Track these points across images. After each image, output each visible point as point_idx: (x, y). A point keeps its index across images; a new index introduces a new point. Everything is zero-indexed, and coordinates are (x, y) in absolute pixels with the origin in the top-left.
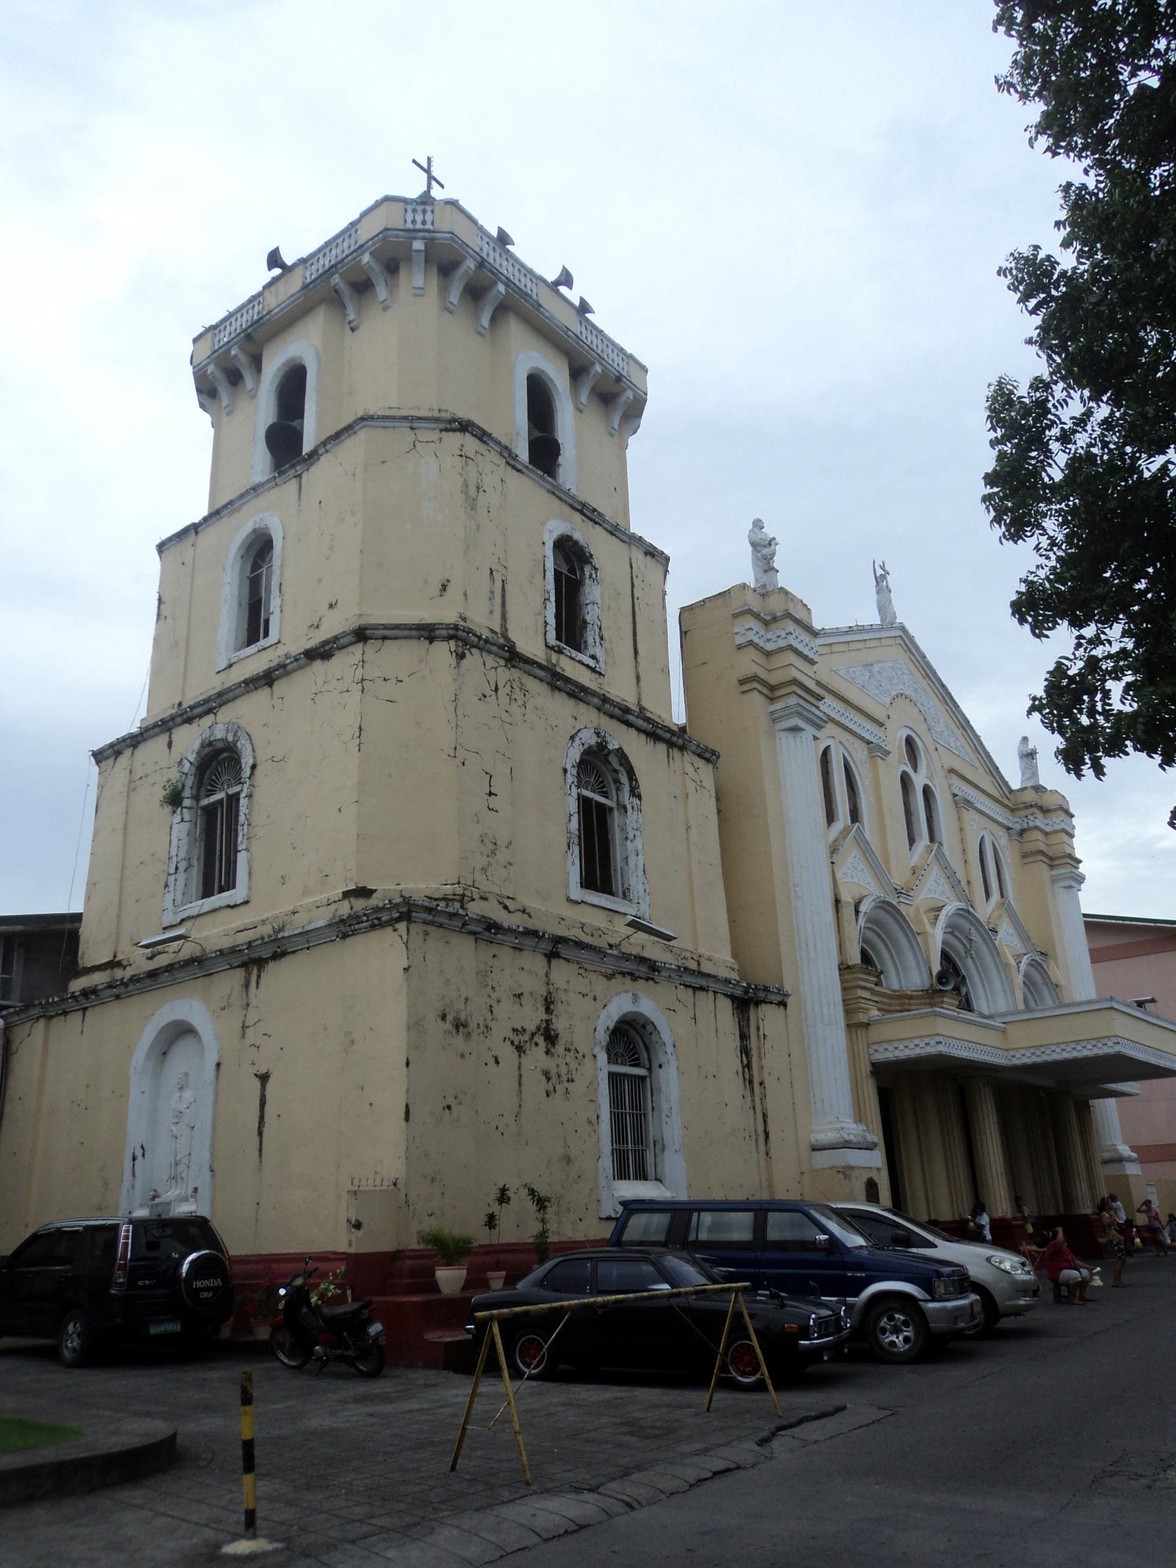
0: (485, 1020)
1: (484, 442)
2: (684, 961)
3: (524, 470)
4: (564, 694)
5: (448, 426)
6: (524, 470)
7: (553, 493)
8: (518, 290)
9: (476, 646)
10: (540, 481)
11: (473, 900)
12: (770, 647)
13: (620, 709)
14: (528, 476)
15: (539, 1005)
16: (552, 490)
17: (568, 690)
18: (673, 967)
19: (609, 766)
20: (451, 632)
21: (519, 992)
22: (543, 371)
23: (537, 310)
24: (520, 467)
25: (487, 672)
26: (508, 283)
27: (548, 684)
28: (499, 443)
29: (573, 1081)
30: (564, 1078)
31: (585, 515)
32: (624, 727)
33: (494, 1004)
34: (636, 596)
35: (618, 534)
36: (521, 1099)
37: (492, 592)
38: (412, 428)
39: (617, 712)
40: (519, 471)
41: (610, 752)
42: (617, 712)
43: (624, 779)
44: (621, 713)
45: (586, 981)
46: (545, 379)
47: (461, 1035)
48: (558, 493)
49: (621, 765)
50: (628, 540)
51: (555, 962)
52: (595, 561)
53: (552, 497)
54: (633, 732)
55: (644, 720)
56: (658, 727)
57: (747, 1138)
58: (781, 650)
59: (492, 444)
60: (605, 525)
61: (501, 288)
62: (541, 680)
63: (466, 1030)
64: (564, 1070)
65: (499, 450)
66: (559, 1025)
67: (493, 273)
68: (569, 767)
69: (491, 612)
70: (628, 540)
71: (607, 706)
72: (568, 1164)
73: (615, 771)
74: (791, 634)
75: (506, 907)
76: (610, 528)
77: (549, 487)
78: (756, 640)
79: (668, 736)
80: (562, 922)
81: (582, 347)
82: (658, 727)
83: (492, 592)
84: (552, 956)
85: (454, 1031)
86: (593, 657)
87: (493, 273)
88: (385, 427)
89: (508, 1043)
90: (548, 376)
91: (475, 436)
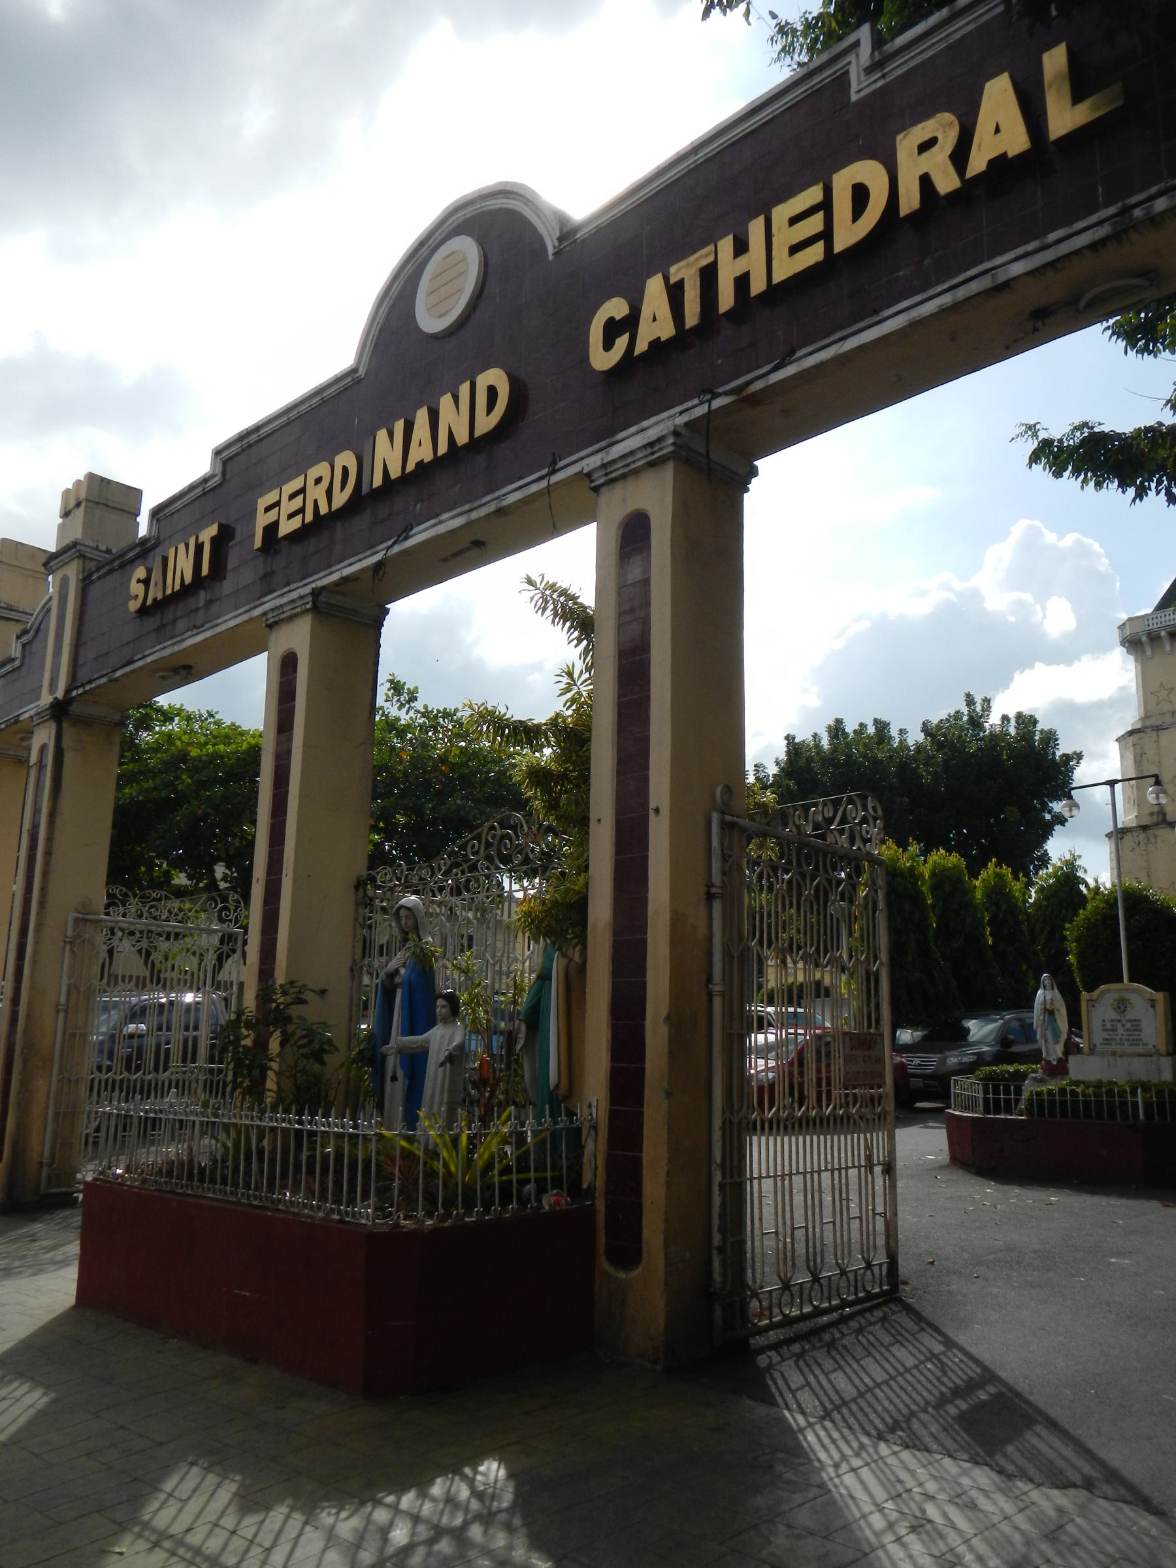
61: (1163, 634)
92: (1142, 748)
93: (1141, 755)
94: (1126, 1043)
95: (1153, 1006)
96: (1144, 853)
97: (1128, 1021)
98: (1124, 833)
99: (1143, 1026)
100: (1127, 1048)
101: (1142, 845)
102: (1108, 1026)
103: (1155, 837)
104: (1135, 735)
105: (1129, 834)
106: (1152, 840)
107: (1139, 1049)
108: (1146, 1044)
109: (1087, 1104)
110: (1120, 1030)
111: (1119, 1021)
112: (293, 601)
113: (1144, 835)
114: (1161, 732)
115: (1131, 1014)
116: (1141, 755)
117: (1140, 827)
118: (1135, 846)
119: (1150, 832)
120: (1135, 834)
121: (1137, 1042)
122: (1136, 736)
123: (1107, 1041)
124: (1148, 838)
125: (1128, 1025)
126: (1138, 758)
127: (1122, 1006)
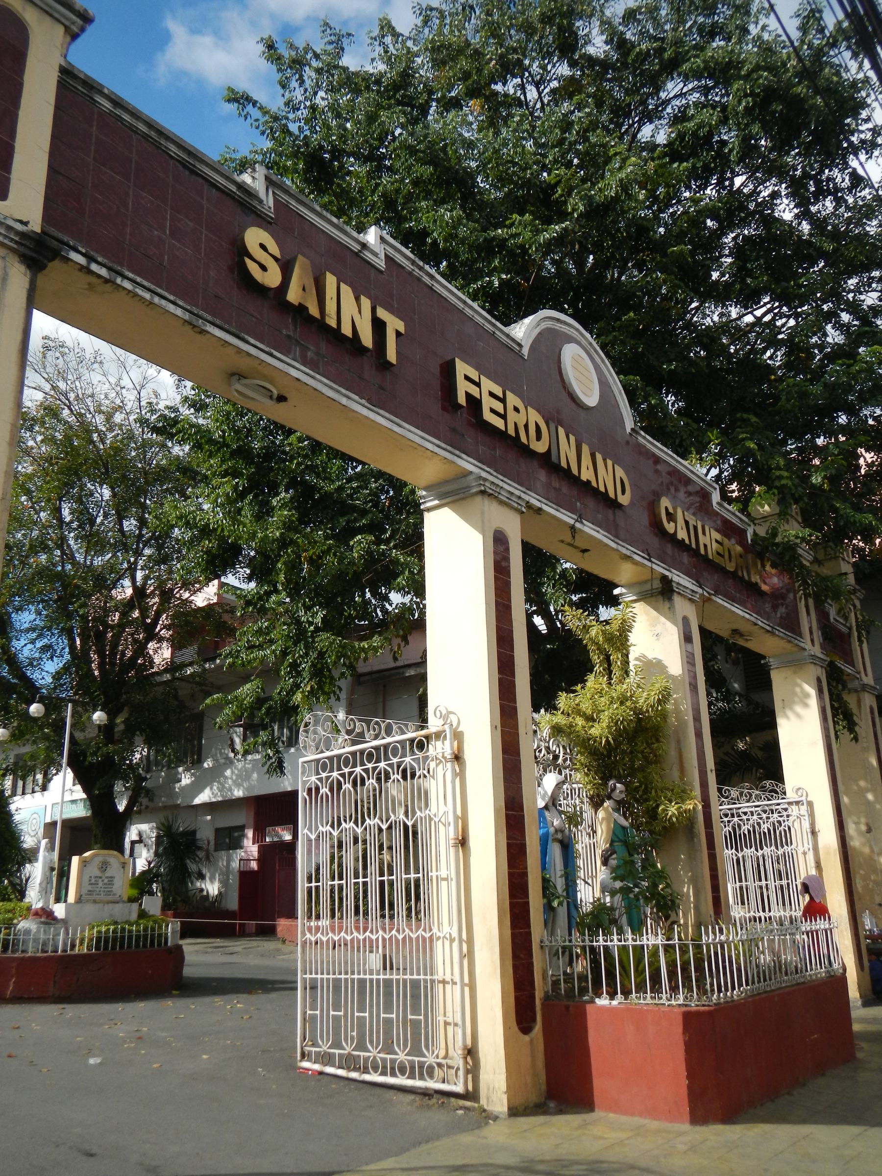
94: (102, 894)
95: (123, 867)
97: (107, 877)
99: (116, 881)
100: (102, 897)
102: (93, 881)
107: (110, 898)
108: (114, 895)
109: (138, 937)
110: (100, 884)
111: (100, 877)
112: (512, 494)
115: (109, 873)
121: (109, 893)
123: (90, 892)
125: (106, 881)
127: (104, 866)
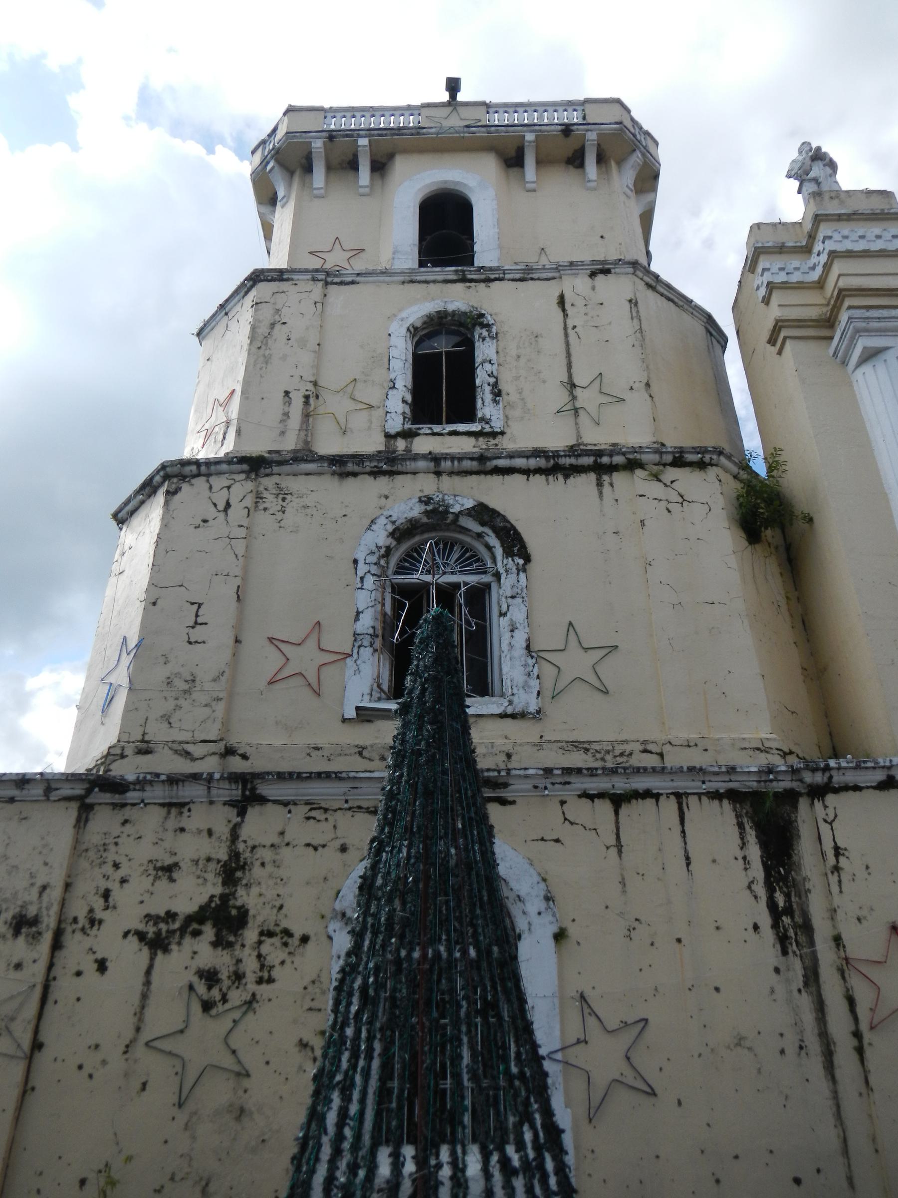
0: (91, 911)
1: (287, 280)
2: (620, 760)
3: (358, 279)
4: (367, 476)
5: (246, 289)
6: (358, 279)
7: (412, 282)
8: (384, 132)
9: (199, 475)
10: (388, 279)
11: (122, 756)
12: (815, 276)
13: (472, 459)
14: (367, 283)
15: (210, 876)
16: (408, 278)
17: (368, 469)
18: (531, 772)
19: (471, 533)
20: (162, 473)
21: (168, 861)
22: (446, 182)
23: (418, 134)
24: (349, 279)
25: (212, 495)
26: (369, 132)
27: (334, 473)
28: (306, 271)
29: (270, 980)
30: (250, 978)
31: (471, 281)
32: (497, 479)
33: (114, 886)
34: (570, 326)
35: (535, 276)
36: (141, 1020)
37: (286, 415)
38: (226, 314)
39: (474, 465)
40: (353, 283)
41: (457, 516)
42: (474, 465)
43: (493, 541)
44: (475, 463)
45: (328, 826)
46: (452, 187)
47: (21, 939)
48: (418, 278)
49: (483, 524)
50: (556, 275)
51: (253, 813)
52: (489, 319)
53: (411, 285)
54: (519, 478)
55: (528, 457)
56: (559, 456)
57: (791, 1050)
58: (827, 267)
59: (295, 277)
60: (507, 276)
61: (363, 142)
62: (320, 474)
63: (34, 929)
64: (250, 965)
65: (309, 277)
66: (245, 897)
67: (347, 136)
68: (361, 556)
69: (283, 433)
70: (556, 275)
71: (446, 465)
72: (238, 1118)
73: (479, 536)
74: (830, 237)
75: (187, 754)
76: (518, 276)
77: (401, 278)
78: (781, 278)
79: (588, 461)
80: (315, 753)
81: (497, 132)
82: (559, 456)
83: (286, 415)
84: (241, 807)
85: (9, 935)
86: (483, 420)
87: (347, 136)
88: (212, 329)
89: (133, 940)
90: (453, 182)
91: (273, 280)
92: (278, 311)
93: (273, 325)
96: (242, 532)
98: (183, 478)
101: (237, 513)
103: (283, 494)
104: (261, 286)
105: (200, 482)
106: (271, 501)
113: (250, 485)
114: (332, 289)
116: (273, 325)
117: (243, 460)
118: (211, 512)
119: (268, 482)
120: (218, 482)
122: (263, 290)
124: (259, 497)
126: (263, 330)
